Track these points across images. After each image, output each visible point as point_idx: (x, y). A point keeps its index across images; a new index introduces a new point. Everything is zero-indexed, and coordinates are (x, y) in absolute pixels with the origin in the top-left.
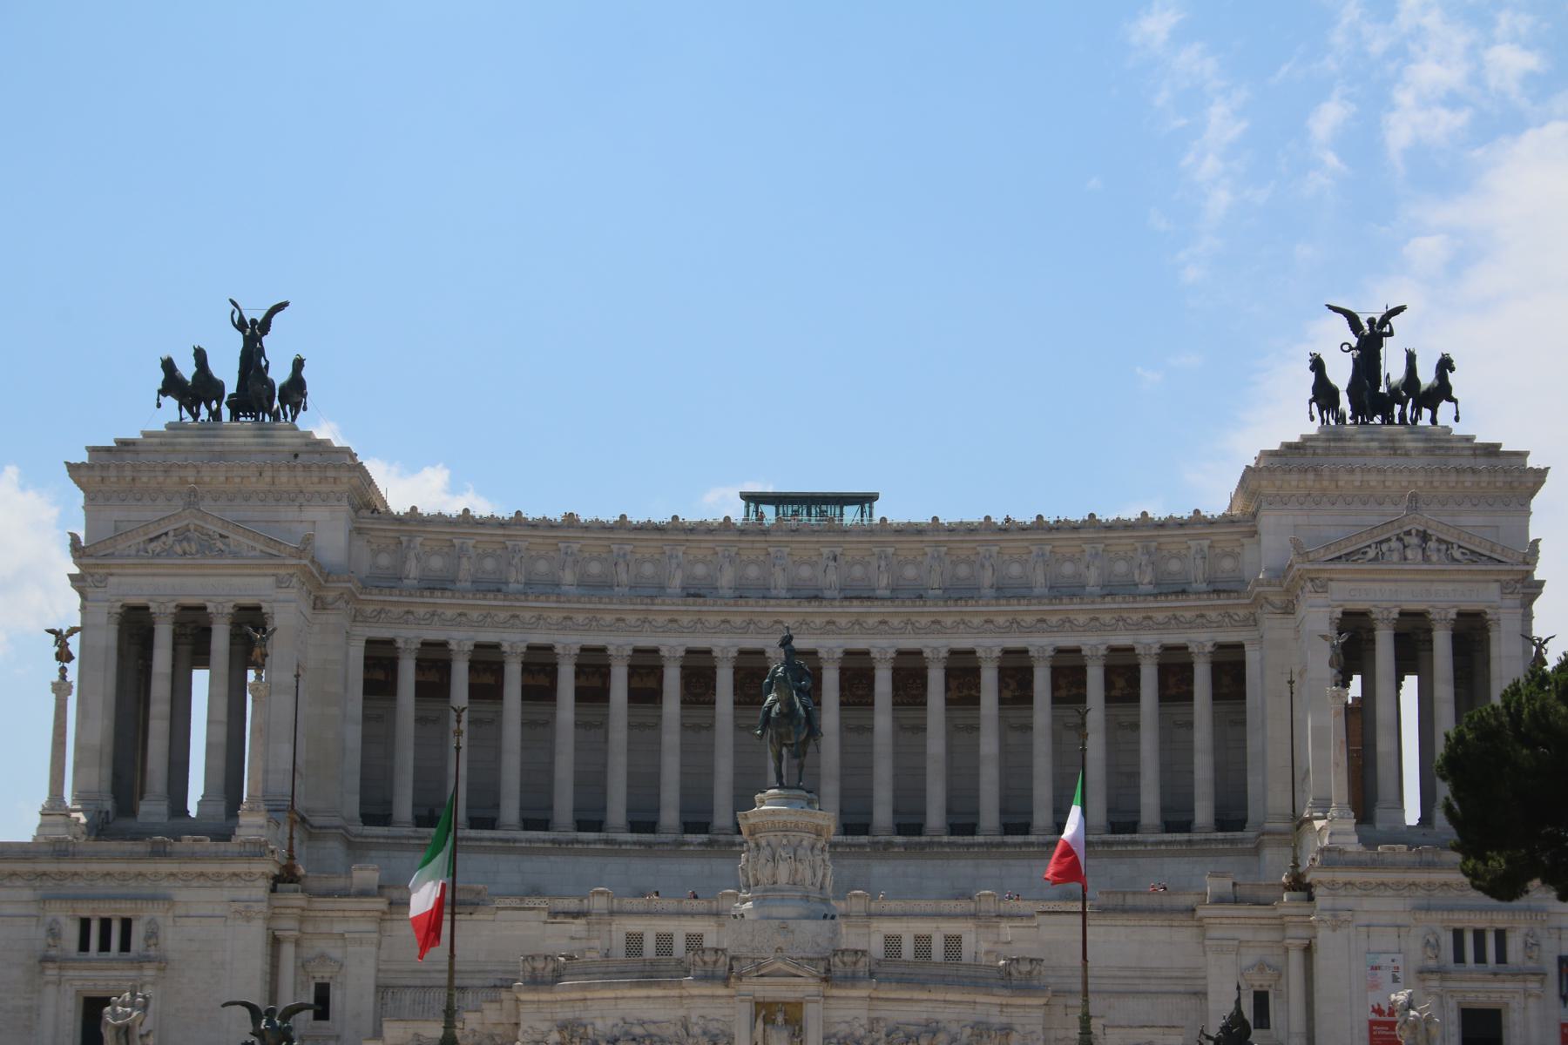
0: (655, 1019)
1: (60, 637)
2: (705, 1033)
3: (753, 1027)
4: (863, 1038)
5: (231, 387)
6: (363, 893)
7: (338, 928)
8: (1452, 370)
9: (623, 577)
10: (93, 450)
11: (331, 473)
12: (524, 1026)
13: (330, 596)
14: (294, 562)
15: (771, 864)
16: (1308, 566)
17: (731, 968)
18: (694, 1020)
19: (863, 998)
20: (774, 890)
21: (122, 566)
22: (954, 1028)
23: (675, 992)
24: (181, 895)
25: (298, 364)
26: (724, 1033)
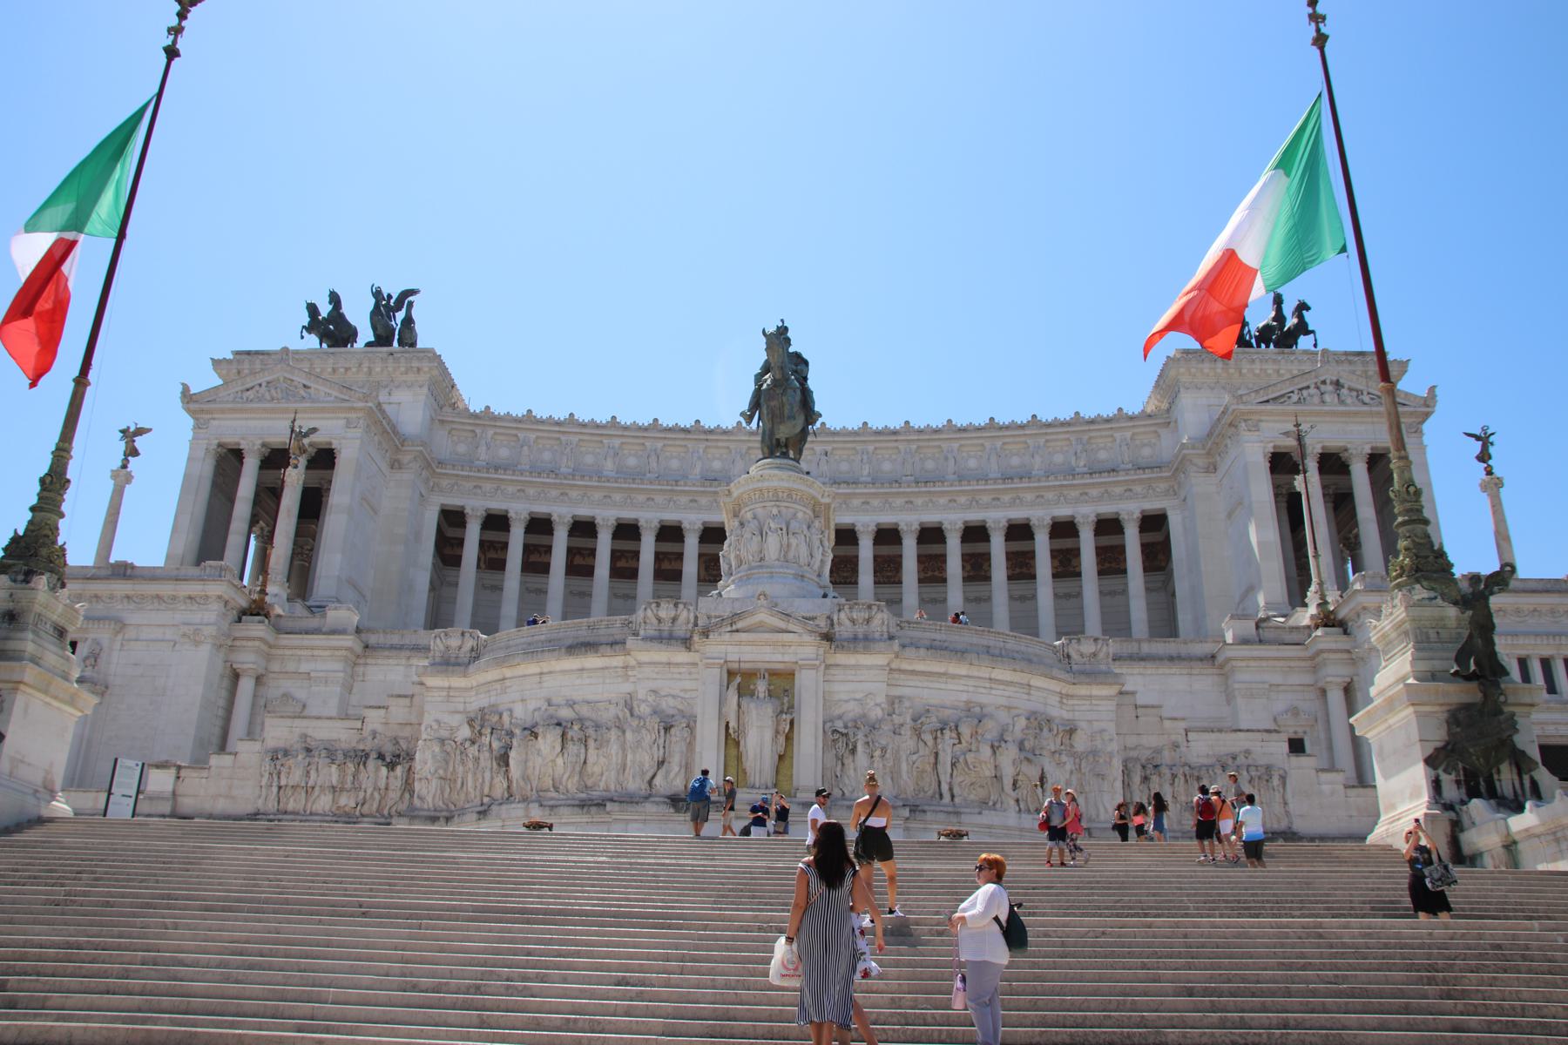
0: (591, 697)
1: (130, 436)
2: (655, 712)
3: (722, 702)
4: (880, 721)
5: (365, 334)
6: (333, 632)
7: (304, 667)
8: (1308, 309)
10: (237, 353)
11: (415, 364)
12: (428, 719)
13: (406, 459)
14: (361, 405)
16: (1241, 407)
17: (696, 625)
18: (641, 694)
19: (881, 668)
21: (222, 411)
22: (1003, 717)
23: (618, 661)
24: (133, 618)
25: (411, 304)
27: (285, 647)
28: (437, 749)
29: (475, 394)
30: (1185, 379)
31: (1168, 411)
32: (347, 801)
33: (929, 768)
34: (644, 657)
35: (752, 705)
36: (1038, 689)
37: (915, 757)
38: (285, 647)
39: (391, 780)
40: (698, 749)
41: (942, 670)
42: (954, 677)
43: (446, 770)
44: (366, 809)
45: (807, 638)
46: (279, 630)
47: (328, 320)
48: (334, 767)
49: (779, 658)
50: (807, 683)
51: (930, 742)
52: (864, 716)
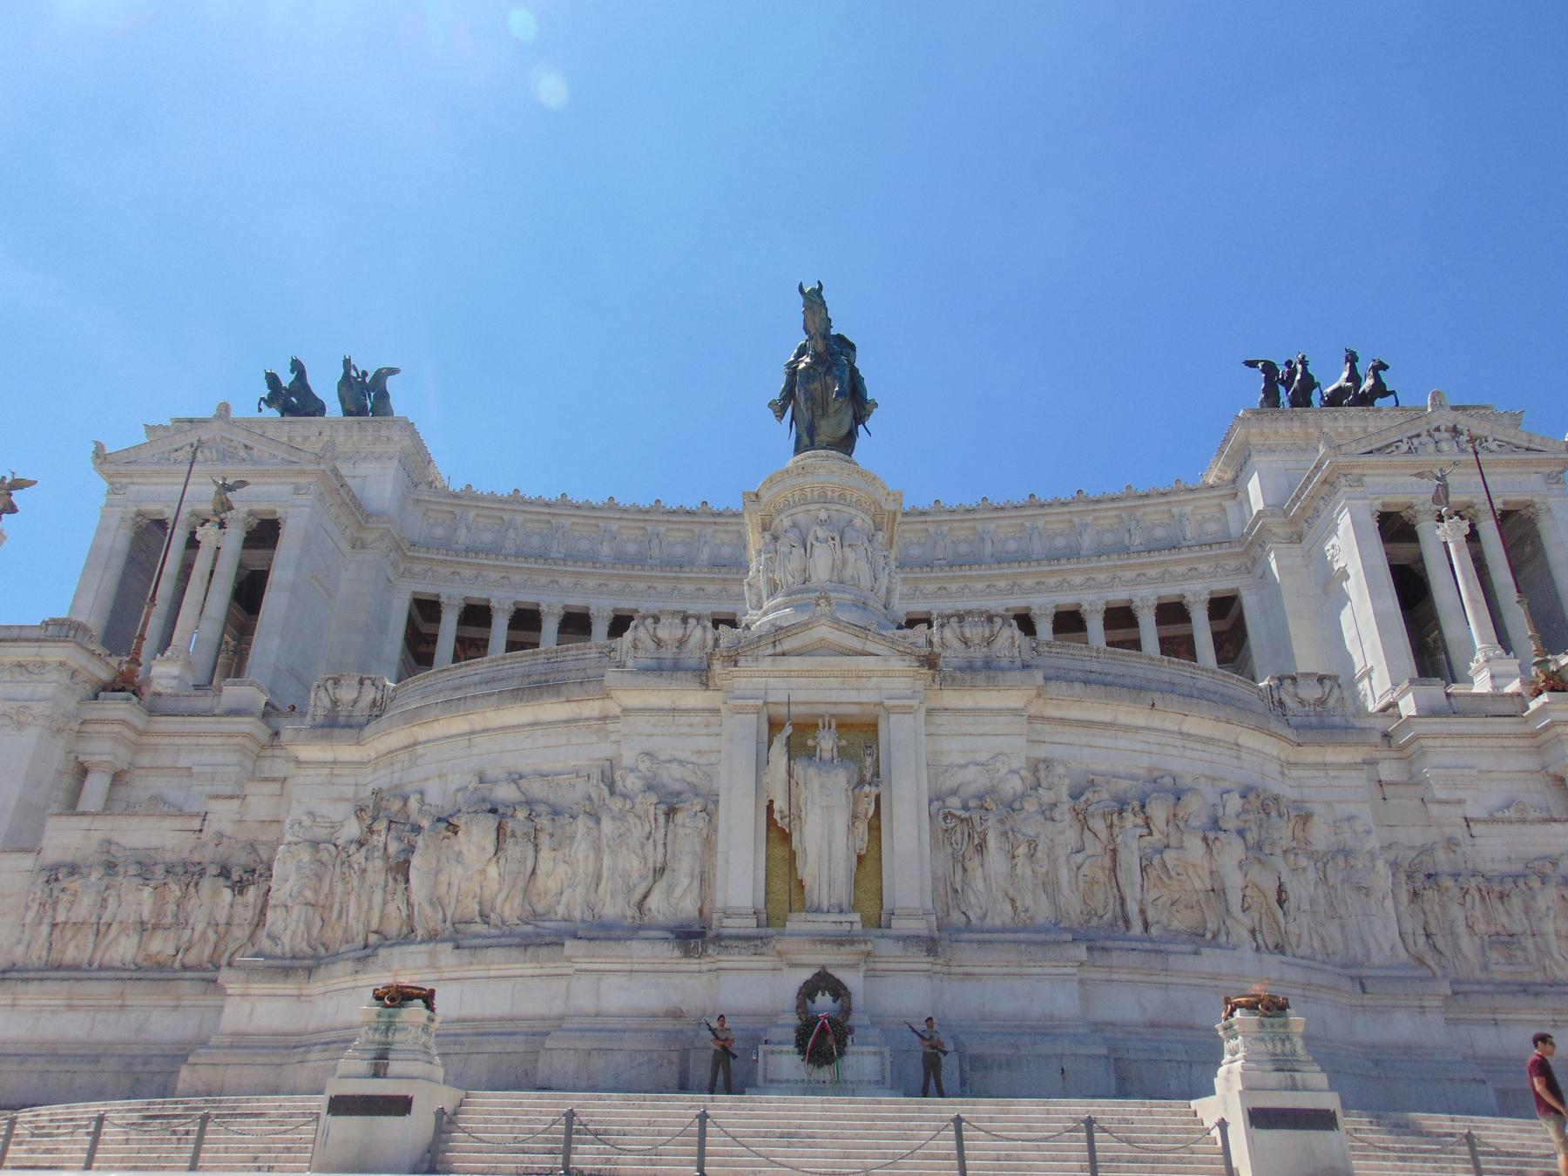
0: (546, 767)
2: (650, 788)
4: (1023, 796)
5: (334, 408)
7: (184, 761)
8: (1384, 367)
9: (656, 551)
11: (384, 432)
13: (370, 537)
14: (312, 467)
15: (799, 551)
16: (1341, 459)
19: (1016, 712)
20: (807, 591)
23: (592, 708)
26: (696, 791)
27: (158, 734)
28: (306, 858)
29: (454, 467)
30: (1256, 440)
31: (1234, 481)
32: (161, 945)
33: (1101, 877)
34: (633, 699)
35: (812, 771)
36: (1251, 751)
37: (1079, 858)
38: (158, 734)
39: (238, 908)
40: (721, 846)
41: (1108, 719)
42: (1128, 728)
43: (316, 891)
44: (191, 958)
45: (897, 664)
46: (152, 711)
47: (291, 391)
48: (147, 891)
49: (853, 696)
50: (899, 734)
51: (1103, 834)
52: (993, 790)
